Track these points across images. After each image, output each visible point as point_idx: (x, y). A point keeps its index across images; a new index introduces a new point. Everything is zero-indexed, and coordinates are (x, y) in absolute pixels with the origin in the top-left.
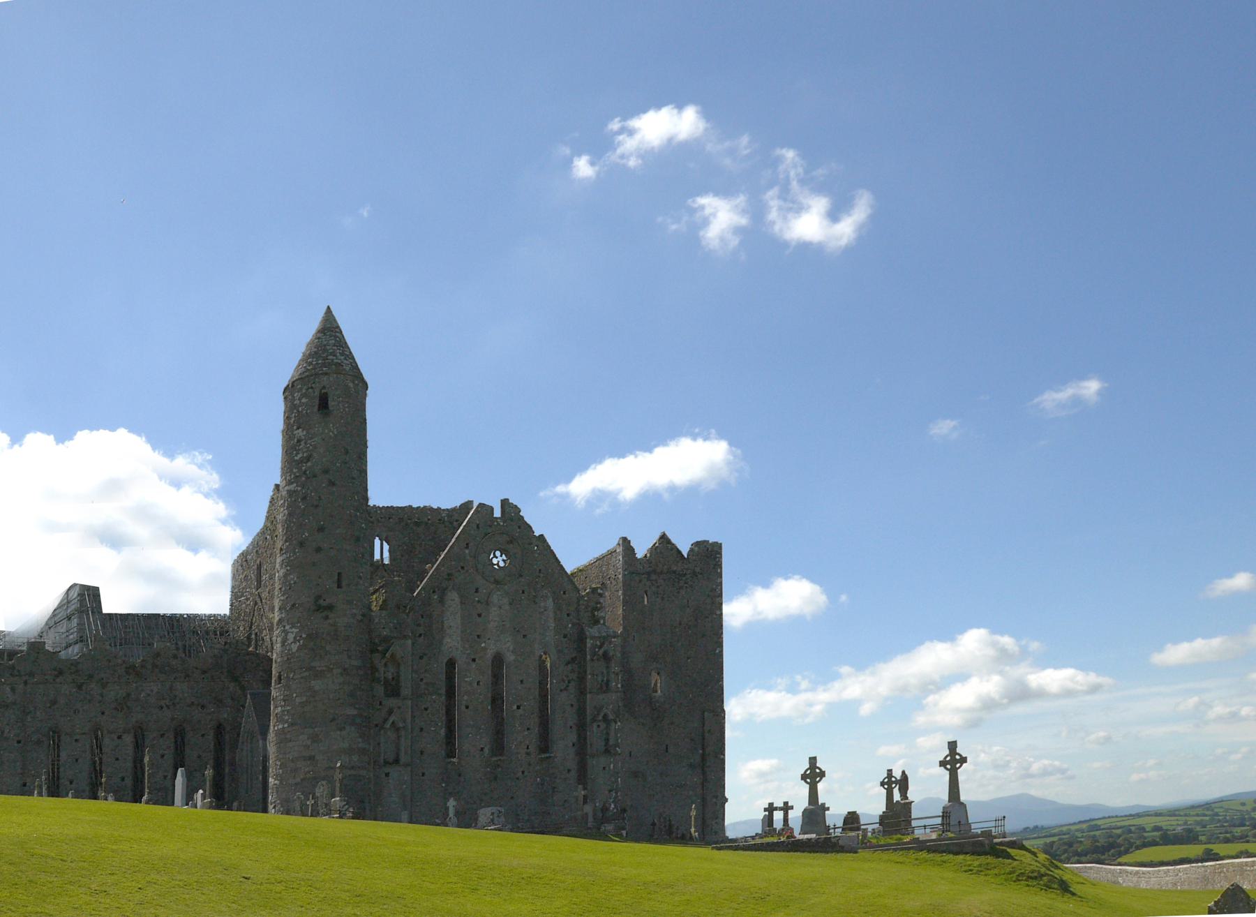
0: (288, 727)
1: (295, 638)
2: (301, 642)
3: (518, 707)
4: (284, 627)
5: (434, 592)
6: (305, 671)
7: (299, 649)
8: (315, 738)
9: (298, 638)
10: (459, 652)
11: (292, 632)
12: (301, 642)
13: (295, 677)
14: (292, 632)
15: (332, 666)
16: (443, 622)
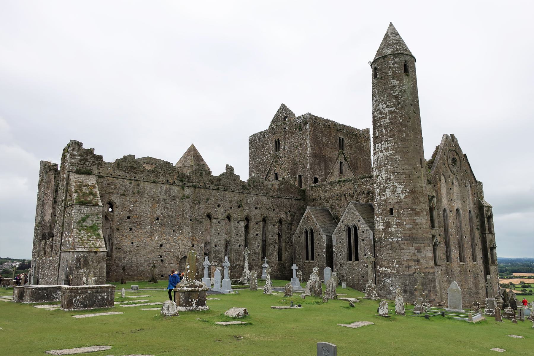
0: (401, 240)
1: (402, 191)
2: (407, 194)
3: (465, 237)
4: (393, 183)
5: (437, 174)
6: (410, 210)
7: (405, 198)
8: (418, 250)
9: (404, 191)
10: (447, 207)
11: (400, 188)
12: (407, 194)
13: (404, 213)
14: (400, 188)
15: (423, 210)
16: (441, 191)
